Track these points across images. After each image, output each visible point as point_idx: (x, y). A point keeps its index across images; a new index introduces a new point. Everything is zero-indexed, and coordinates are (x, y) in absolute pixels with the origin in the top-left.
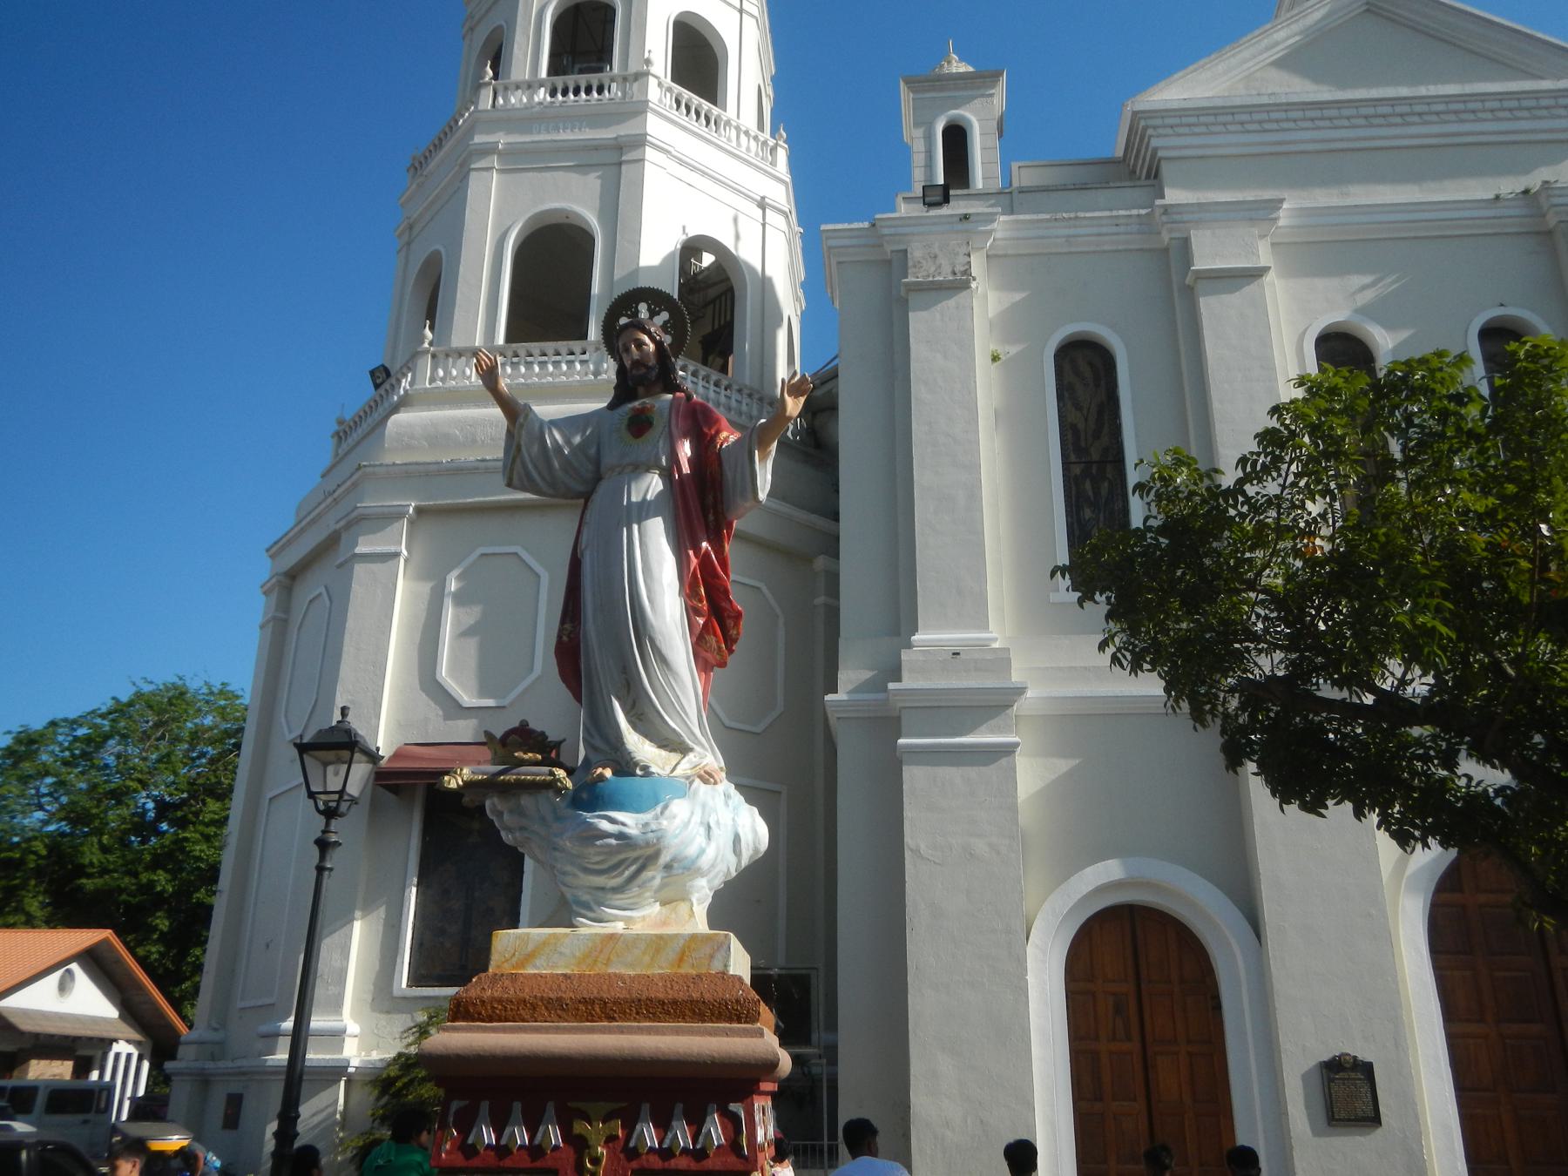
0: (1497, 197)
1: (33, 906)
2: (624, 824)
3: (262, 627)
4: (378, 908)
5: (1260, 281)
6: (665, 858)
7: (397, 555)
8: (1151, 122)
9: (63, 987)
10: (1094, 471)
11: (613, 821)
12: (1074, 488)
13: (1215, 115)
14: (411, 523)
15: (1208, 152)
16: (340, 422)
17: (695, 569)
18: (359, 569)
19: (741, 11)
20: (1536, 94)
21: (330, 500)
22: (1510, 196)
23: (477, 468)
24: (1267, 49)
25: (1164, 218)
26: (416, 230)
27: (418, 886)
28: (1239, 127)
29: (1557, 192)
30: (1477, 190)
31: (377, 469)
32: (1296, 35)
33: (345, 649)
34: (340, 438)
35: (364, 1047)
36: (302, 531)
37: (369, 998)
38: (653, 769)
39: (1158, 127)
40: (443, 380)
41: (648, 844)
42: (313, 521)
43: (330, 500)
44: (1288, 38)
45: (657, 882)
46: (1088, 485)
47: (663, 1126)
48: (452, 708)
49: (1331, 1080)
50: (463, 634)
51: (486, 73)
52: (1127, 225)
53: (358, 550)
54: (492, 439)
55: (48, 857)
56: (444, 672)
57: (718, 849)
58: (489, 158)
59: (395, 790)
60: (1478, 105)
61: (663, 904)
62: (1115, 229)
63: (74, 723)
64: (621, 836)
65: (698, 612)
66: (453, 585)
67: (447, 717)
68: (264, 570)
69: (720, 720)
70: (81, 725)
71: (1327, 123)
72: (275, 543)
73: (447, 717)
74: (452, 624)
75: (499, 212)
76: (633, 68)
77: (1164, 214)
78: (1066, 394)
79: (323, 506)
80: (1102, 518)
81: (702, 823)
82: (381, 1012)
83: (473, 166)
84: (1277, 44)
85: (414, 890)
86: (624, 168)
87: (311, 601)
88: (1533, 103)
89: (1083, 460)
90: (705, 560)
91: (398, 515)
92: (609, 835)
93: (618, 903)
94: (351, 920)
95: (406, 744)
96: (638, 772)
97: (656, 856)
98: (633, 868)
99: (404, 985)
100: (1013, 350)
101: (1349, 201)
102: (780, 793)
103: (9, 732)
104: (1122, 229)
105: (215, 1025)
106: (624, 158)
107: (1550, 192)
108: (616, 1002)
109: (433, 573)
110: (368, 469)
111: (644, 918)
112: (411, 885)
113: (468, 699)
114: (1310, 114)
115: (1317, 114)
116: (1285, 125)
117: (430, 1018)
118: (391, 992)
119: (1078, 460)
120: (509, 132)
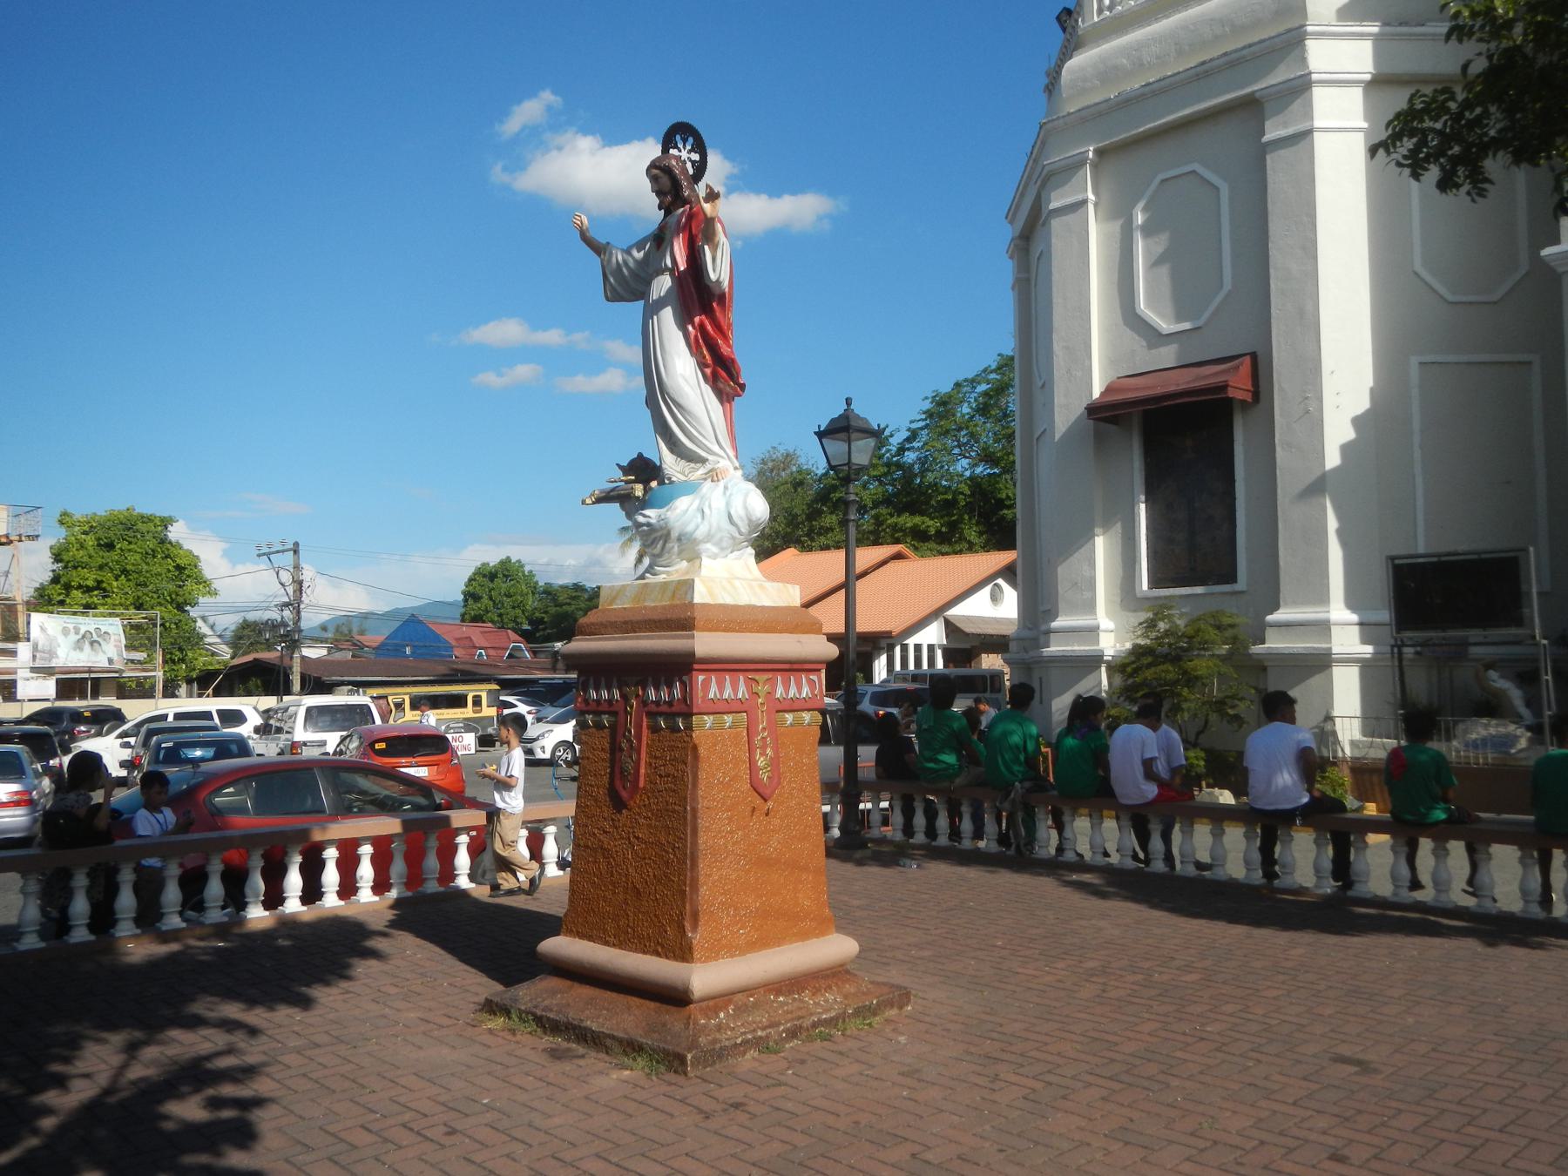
1: (971, 533)
2: (649, 517)
3: (1013, 288)
4: (1116, 522)
6: (674, 535)
7: (1085, 202)
9: (995, 598)
11: (645, 516)
14: (1095, 166)
16: (1048, 75)
17: (696, 336)
18: (1056, 224)
21: (1031, 162)
23: (1143, 95)
27: (1146, 502)
31: (1056, 123)
33: (1054, 301)
34: (1050, 91)
35: (1118, 639)
38: (674, 479)
41: (661, 528)
43: (1031, 162)
45: (676, 549)
47: (657, 689)
48: (1154, 337)
50: (1154, 263)
53: (1054, 205)
54: (1157, 58)
55: (973, 495)
57: (711, 526)
59: (1113, 420)
61: (689, 561)
63: (973, 382)
64: (648, 524)
65: (707, 366)
66: (1140, 218)
67: (1151, 346)
68: (1006, 233)
69: (1441, 297)
70: (979, 383)
72: (1009, 210)
73: (1151, 346)
74: (1144, 257)
79: (1029, 168)
81: (698, 509)
82: (1130, 610)
85: (1143, 506)
87: (1039, 259)
90: (702, 327)
91: (1080, 163)
92: (643, 525)
93: (664, 563)
94: (1092, 537)
95: (1119, 378)
96: (666, 481)
97: (668, 534)
98: (661, 542)
99: (1145, 586)
102: (1530, 363)
103: (927, 398)
105: (1030, 626)
108: (637, 622)
109: (1119, 211)
110: (1049, 126)
111: (677, 571)
112: (1139, 502)
113: (1165, 326)
117: (1155, 614)
118: (1135, 595)
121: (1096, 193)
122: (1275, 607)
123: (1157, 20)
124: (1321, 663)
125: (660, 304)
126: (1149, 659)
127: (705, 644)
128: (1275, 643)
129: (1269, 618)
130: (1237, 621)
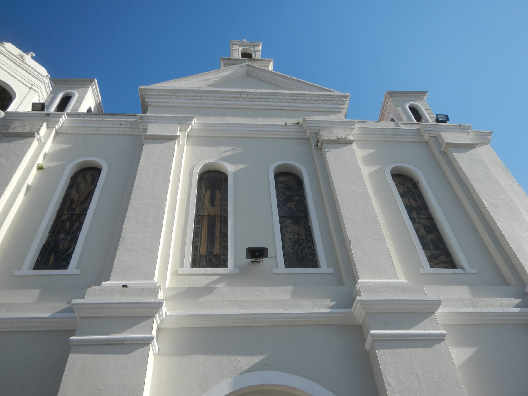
0: (286, 124)
5: (174, 141)
8: (146, 93)
10: (74, 218)
12: (60, 224)
13: (174, 93)
15: (169, 105)
19: (31, 88)
20: (304, 95)
22: (291, 124)
24: (204, 80)
25: (140, 121)
28: (184, 98)
29: (309, 122)
30: (280, 122)
32: (217, 78)
39: (150, 95)
46: (68, 224)
52: (125, 125)
62: (119, 126)
71: (221, 99)
77: (140, 119)
78: (75, 187)
80: (68, 239)
84: (209, 79)
88: (302, 98)
89: (71, 213)
100: (51, 164)
101: (224, 122)
104: (121, 126)
107: (306, 122)
116: (202, 98)
119: (68, 213)
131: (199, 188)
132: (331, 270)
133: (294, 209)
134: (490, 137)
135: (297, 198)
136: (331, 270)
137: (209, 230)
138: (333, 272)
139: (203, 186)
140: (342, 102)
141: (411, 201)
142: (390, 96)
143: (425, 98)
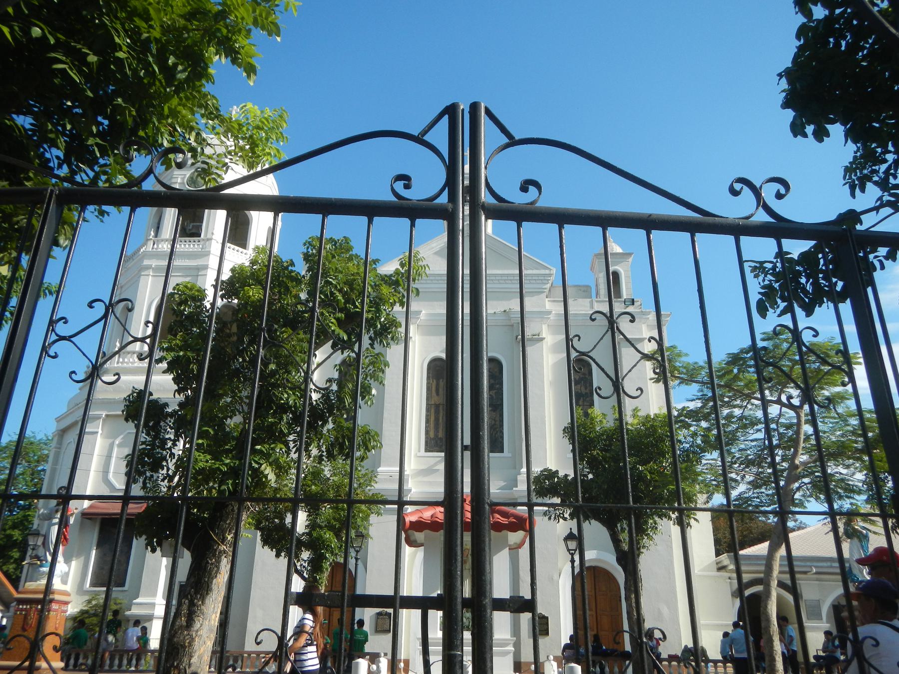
0: (495, 313)
14: (104, 420)
26: (123, 289)
36: (68, 415)
37: (76, 591)
40: (122, 363)
42: (71, 413)
43: (76, 407)
44: (437, 246)
49: (378, 618)
51: (150, 234)
56: (111, 476)
58: (149, 270)
60: (494, 278)
75: (150, 292)
76: (209, 236)
83: (142, 274)
84: (433, 248)
85: (94, 552)
86: (199, 277)
87: (69, 443)
91: (99, 418)
99: (88, 586)
106: (200, 274)
114: (437, 278)
115: (440, 278)
118: (83, 589)
120: (158, 259)
121: (102, 430)
122: (137, 597)
123: (138, 375)
124: (150, 618)
125: (55, 524)
126: (86, 615)
127: (57, 597)
128: (135, 611)
129: (134, 601)
130: (122, 601)
131: (428, 378)
132: (510, 455)
133: (494, 395)
134: (668, 319)
135: (498, 386)
136: (510, 455)
137: (435, 417)
138: (511, 456)
139: (431, 375)
140: (546, 282)
141: (583, 388)
142: (599, 259)
143: (630, 260)
